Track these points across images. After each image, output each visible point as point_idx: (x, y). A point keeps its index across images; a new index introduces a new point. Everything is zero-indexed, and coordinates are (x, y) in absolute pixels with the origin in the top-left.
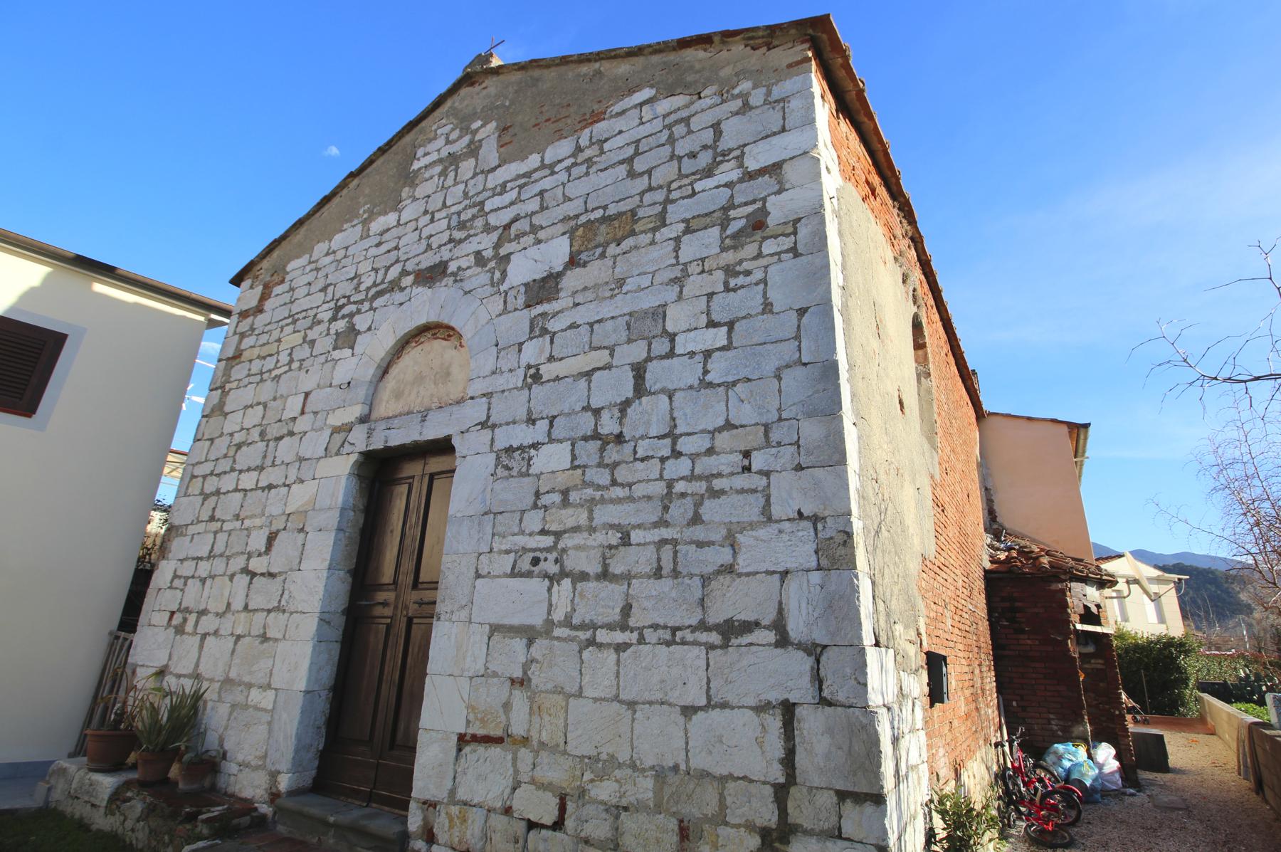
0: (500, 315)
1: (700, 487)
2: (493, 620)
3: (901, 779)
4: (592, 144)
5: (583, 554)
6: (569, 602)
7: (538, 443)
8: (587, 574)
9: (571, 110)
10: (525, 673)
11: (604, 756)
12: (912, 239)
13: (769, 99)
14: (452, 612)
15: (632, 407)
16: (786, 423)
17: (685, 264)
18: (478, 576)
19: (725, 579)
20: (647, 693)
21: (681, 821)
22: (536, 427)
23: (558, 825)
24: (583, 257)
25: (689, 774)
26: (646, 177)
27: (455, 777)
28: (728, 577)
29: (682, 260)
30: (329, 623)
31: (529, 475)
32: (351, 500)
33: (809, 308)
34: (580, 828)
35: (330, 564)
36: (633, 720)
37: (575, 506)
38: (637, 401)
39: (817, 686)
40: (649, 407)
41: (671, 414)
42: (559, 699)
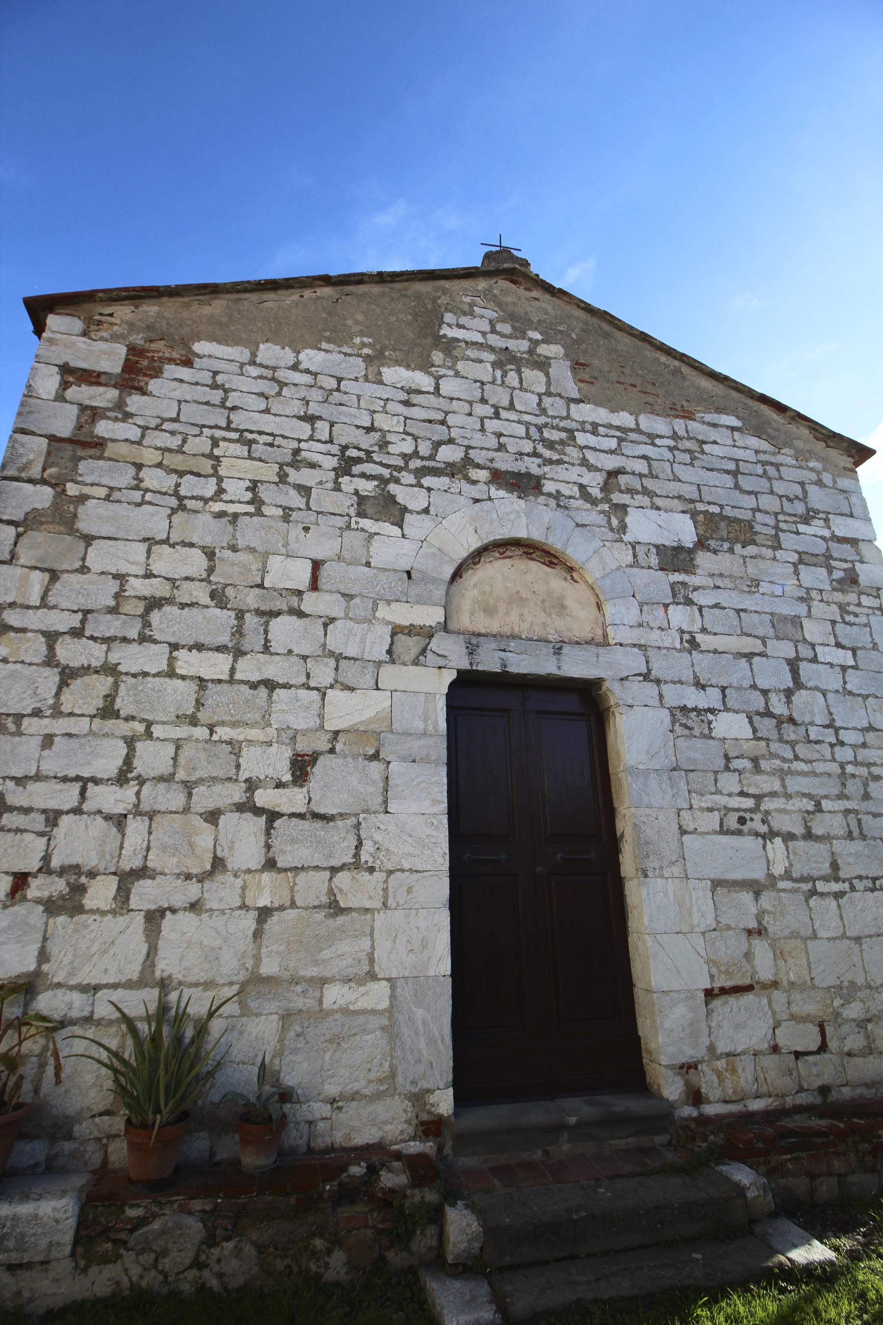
2: (713, 876)
8: (794, 834)
10: (760, 923)
11: (846, 984)
18: (683, 832)
36: (861, 951)
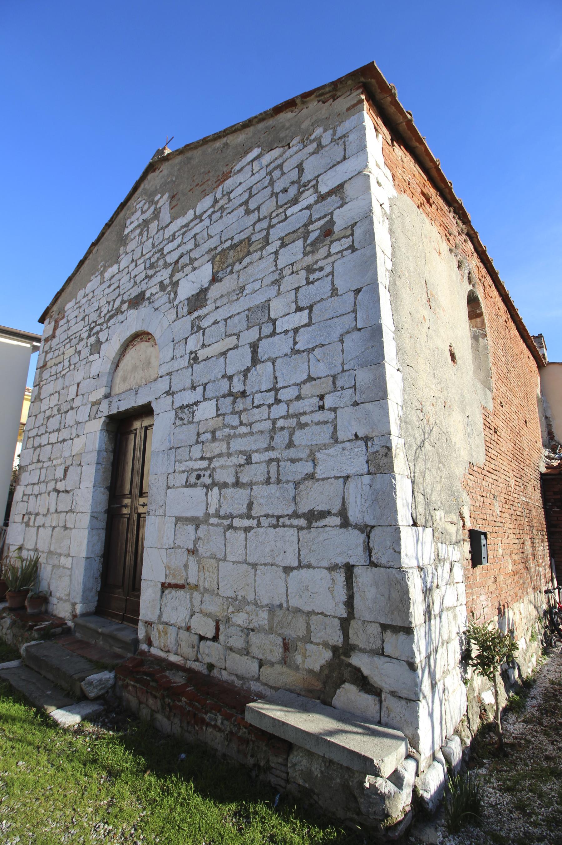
0: (175, 321)
1: (292, 422)
2: (176, 515)
3: (433, 617)
4: (223, 196)
5: (224, 471)
6: (217, 501)
7: (198, 402)
8: (227, 484)
9: (211, 174)
10: (195, 546)
11: (239, 598)
12: (468, 234)
13: (335, 138)
14: (156, 510)
15: (251, 373)
16: (347, 373)
17: (281, 270)
18: (168, 487)
19: (309, 483)
20: (263, 558)
21: (284, 639)
22: (197, 391)
23: (215, 638)
24: (220, 275)
25: (288, 610)
26: (256, 212)
27: (161, 608)
28: (311, 482)
29: (279, 267)
30: (97, 518)
31: (193, 423)
32: (104, 446)
33: (362, 288)
34: (227, 641)
35: (94, 484)
36: (255, 575)
37: (220, 440)
38: (254, 368)
39: (368, 554)
40: (261, 371)
41: (274, 375)
42: (214, 561)
